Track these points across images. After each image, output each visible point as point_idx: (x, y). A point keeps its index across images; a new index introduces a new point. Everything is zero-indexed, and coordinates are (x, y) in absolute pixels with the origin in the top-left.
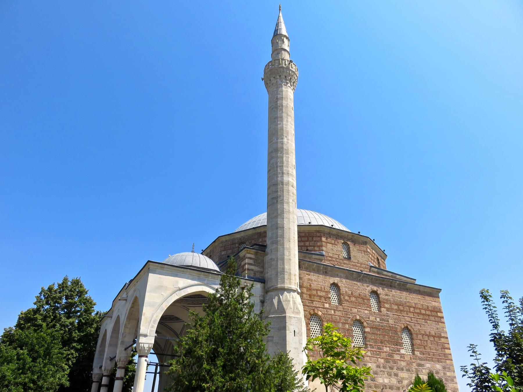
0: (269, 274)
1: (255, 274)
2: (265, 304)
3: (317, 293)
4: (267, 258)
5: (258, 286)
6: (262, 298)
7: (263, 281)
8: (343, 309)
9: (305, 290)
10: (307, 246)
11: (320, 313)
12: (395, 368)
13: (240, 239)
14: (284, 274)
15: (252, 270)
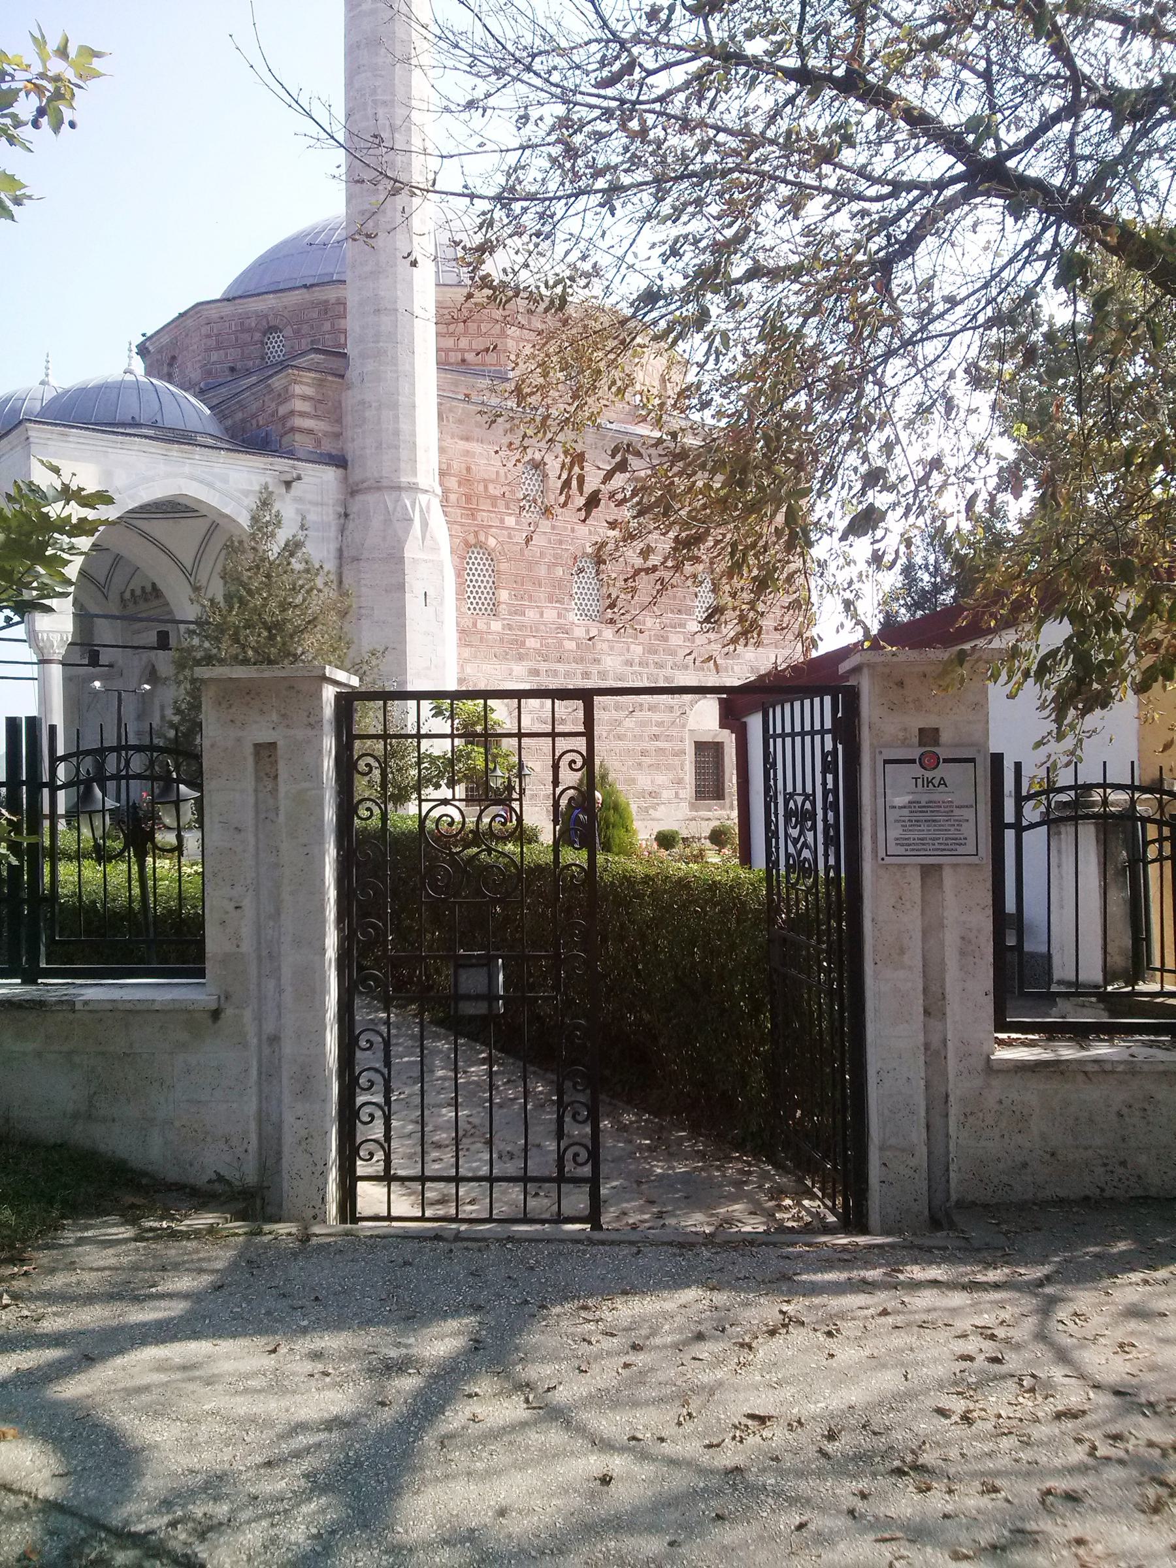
0: (357, 444)
1: (318, 442)
2: (351, 525)
3: (486, 487)
4: (350, 399)
5: (330, 474)
6: (341, 510)
7: (339, 462)
8: (553, 527)
9: (452, 483)
10: (463, 351)
11: (492, 542)
12: (670, 664)
13: (266, 316)
14: (397, 447)
15: (310, 432)
